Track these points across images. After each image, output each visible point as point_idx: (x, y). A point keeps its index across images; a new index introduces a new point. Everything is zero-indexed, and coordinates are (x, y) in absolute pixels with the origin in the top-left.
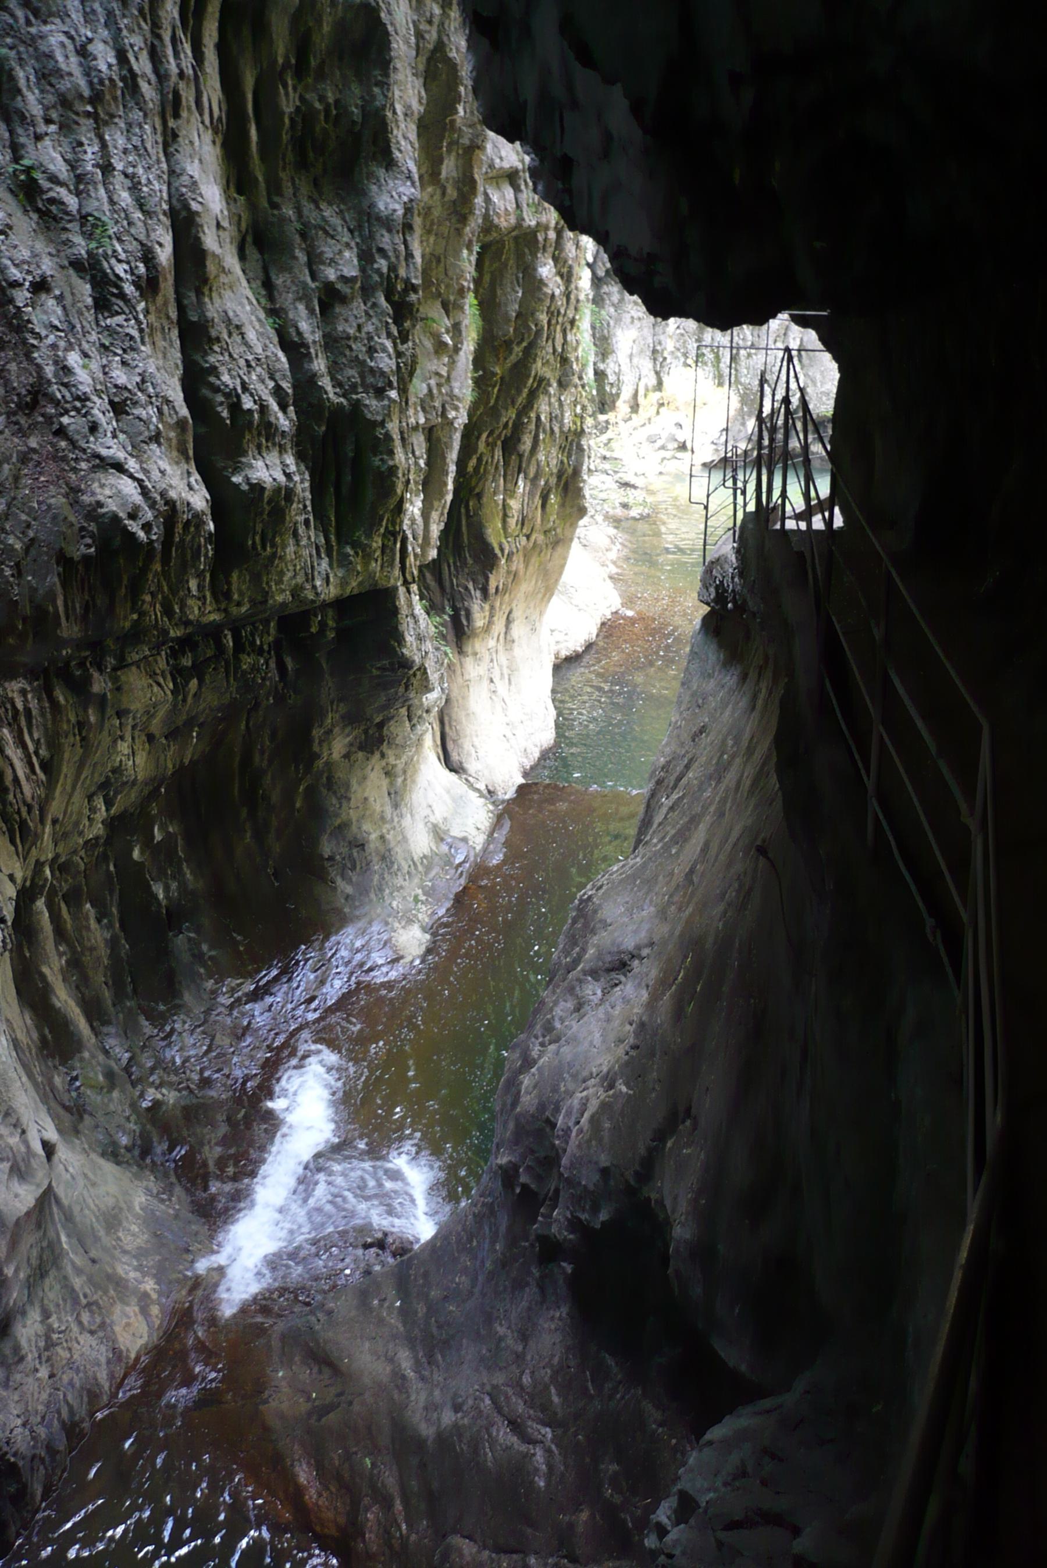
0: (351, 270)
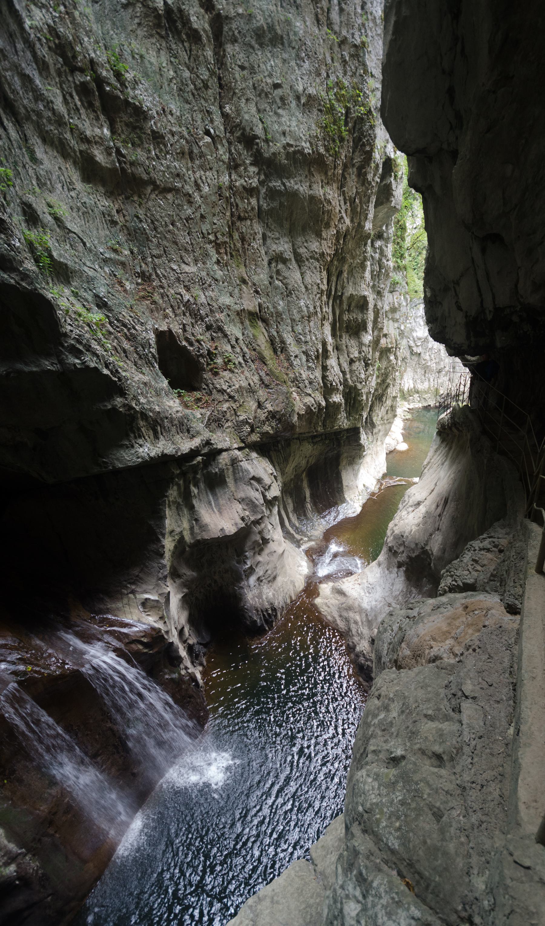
0: (357, 355)
